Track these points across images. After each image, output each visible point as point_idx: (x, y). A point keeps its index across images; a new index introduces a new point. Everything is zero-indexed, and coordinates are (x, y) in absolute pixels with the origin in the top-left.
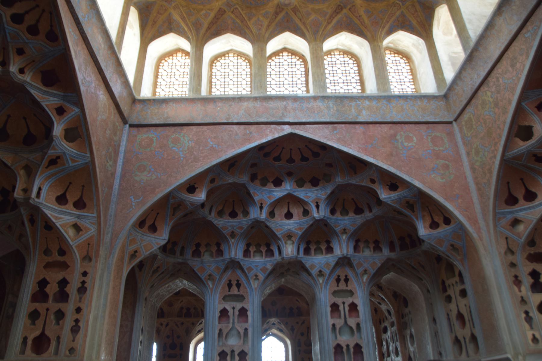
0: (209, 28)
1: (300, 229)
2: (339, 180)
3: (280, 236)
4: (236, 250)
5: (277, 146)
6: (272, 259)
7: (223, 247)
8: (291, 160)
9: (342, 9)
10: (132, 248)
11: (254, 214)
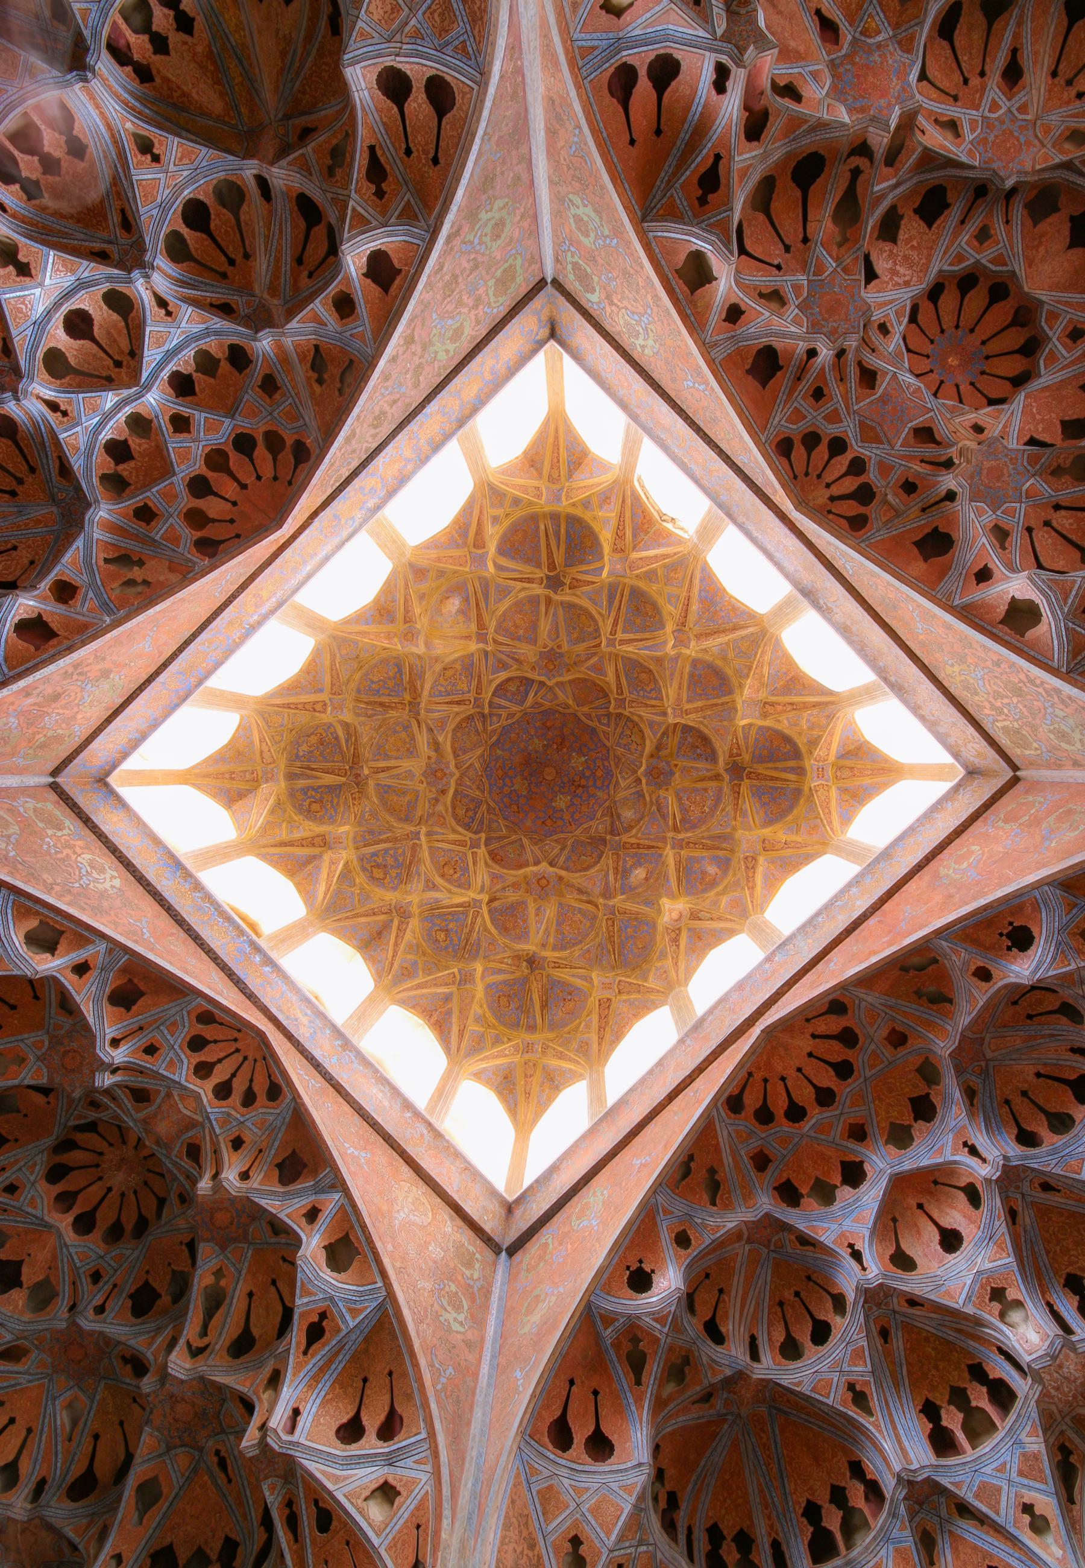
0: (601, 1039)
1: (1001, 1247)
2: (943, 1047)
3: (970, 1310)
4: (899, 1442)
5: (766, 1081)
6: (1018, 1404)
7: (873, 1467)
8: (825, 1097)
9: (754, 859)
10: (558, 1525)
11: (849, 1279)
